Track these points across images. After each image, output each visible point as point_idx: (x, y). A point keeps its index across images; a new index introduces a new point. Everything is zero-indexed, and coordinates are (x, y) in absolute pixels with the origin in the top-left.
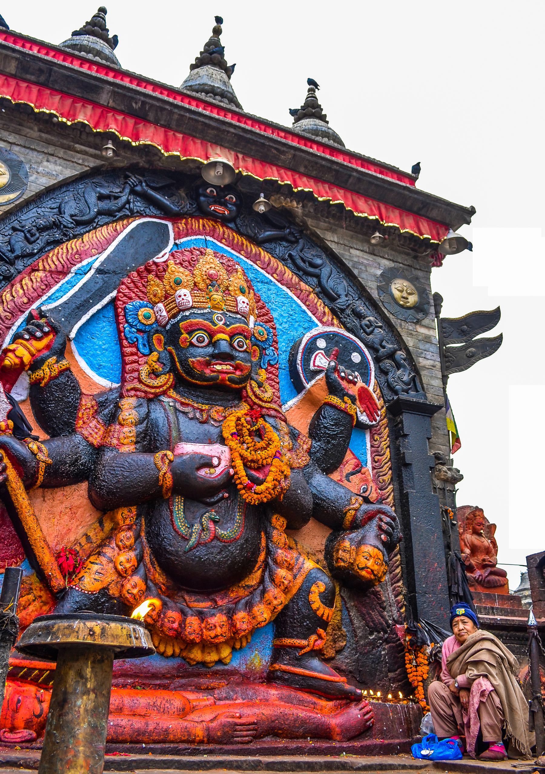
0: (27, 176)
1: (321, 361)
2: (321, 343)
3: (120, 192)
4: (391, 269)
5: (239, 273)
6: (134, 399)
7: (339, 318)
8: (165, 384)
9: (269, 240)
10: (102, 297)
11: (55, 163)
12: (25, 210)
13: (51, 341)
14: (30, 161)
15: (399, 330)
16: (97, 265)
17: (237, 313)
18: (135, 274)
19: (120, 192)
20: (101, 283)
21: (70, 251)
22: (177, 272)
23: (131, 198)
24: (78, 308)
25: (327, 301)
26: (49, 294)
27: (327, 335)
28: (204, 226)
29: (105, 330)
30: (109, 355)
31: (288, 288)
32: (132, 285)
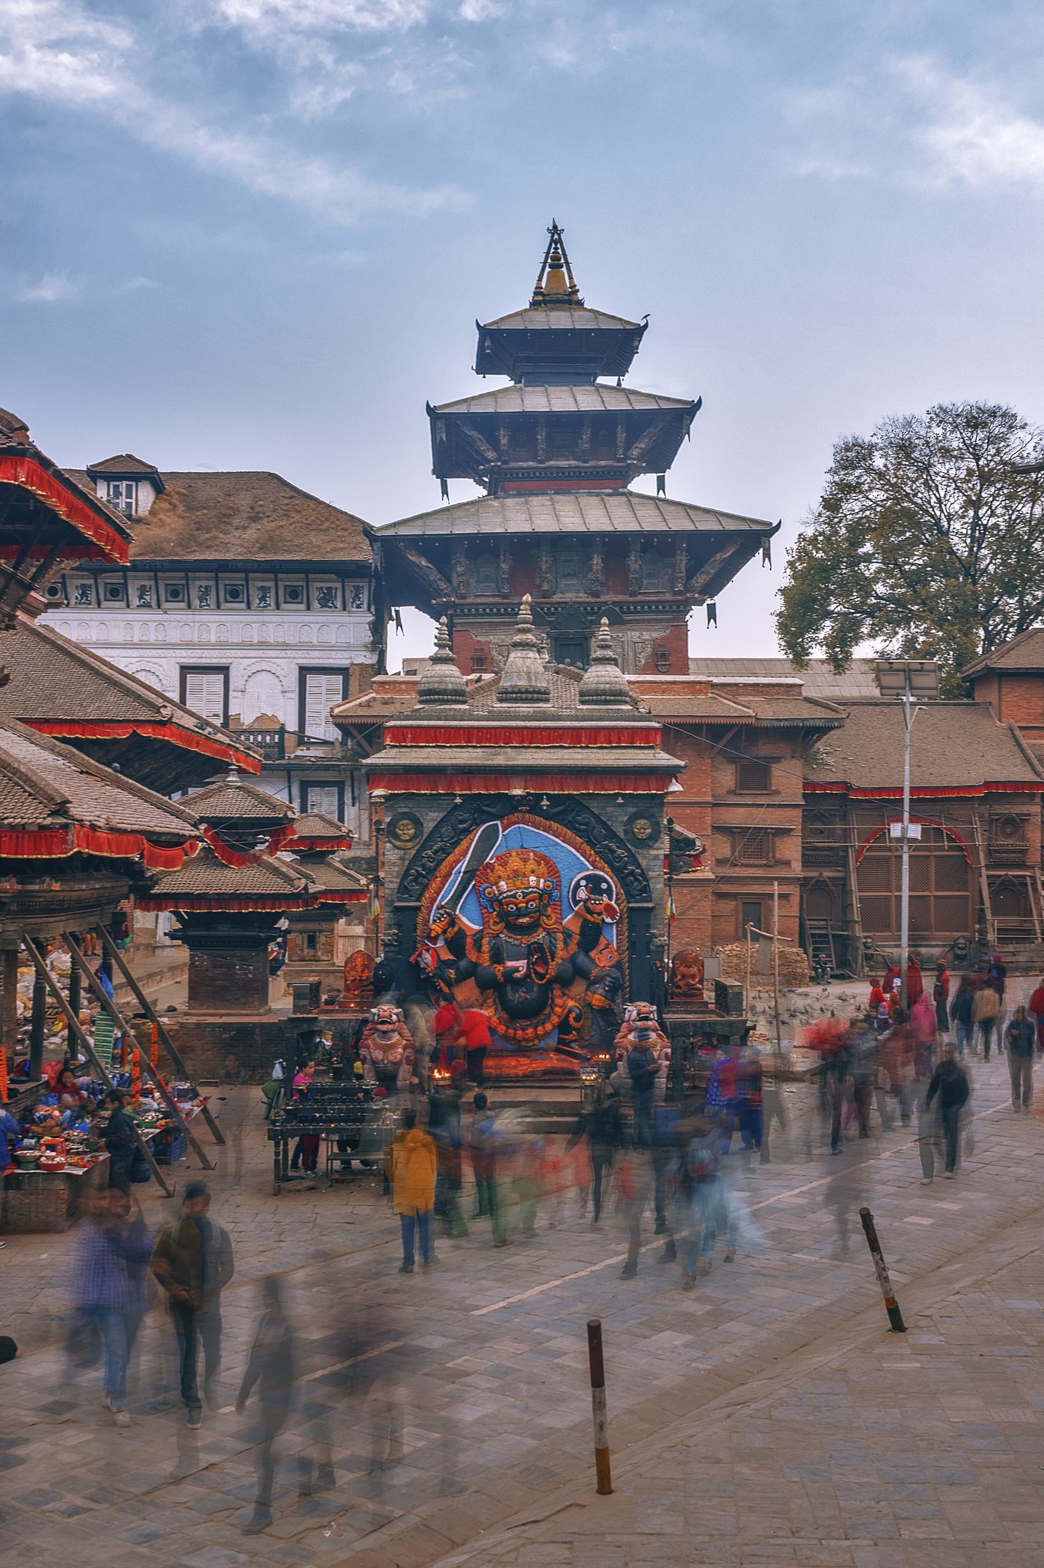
0: (422, 825)
1: (582, 894)
2: (583, 883)
4: (634, 814)
9: (558, 813)
16: (463, 870)
22: (500, 870)
29: (473, 899)
30: (476, 913)
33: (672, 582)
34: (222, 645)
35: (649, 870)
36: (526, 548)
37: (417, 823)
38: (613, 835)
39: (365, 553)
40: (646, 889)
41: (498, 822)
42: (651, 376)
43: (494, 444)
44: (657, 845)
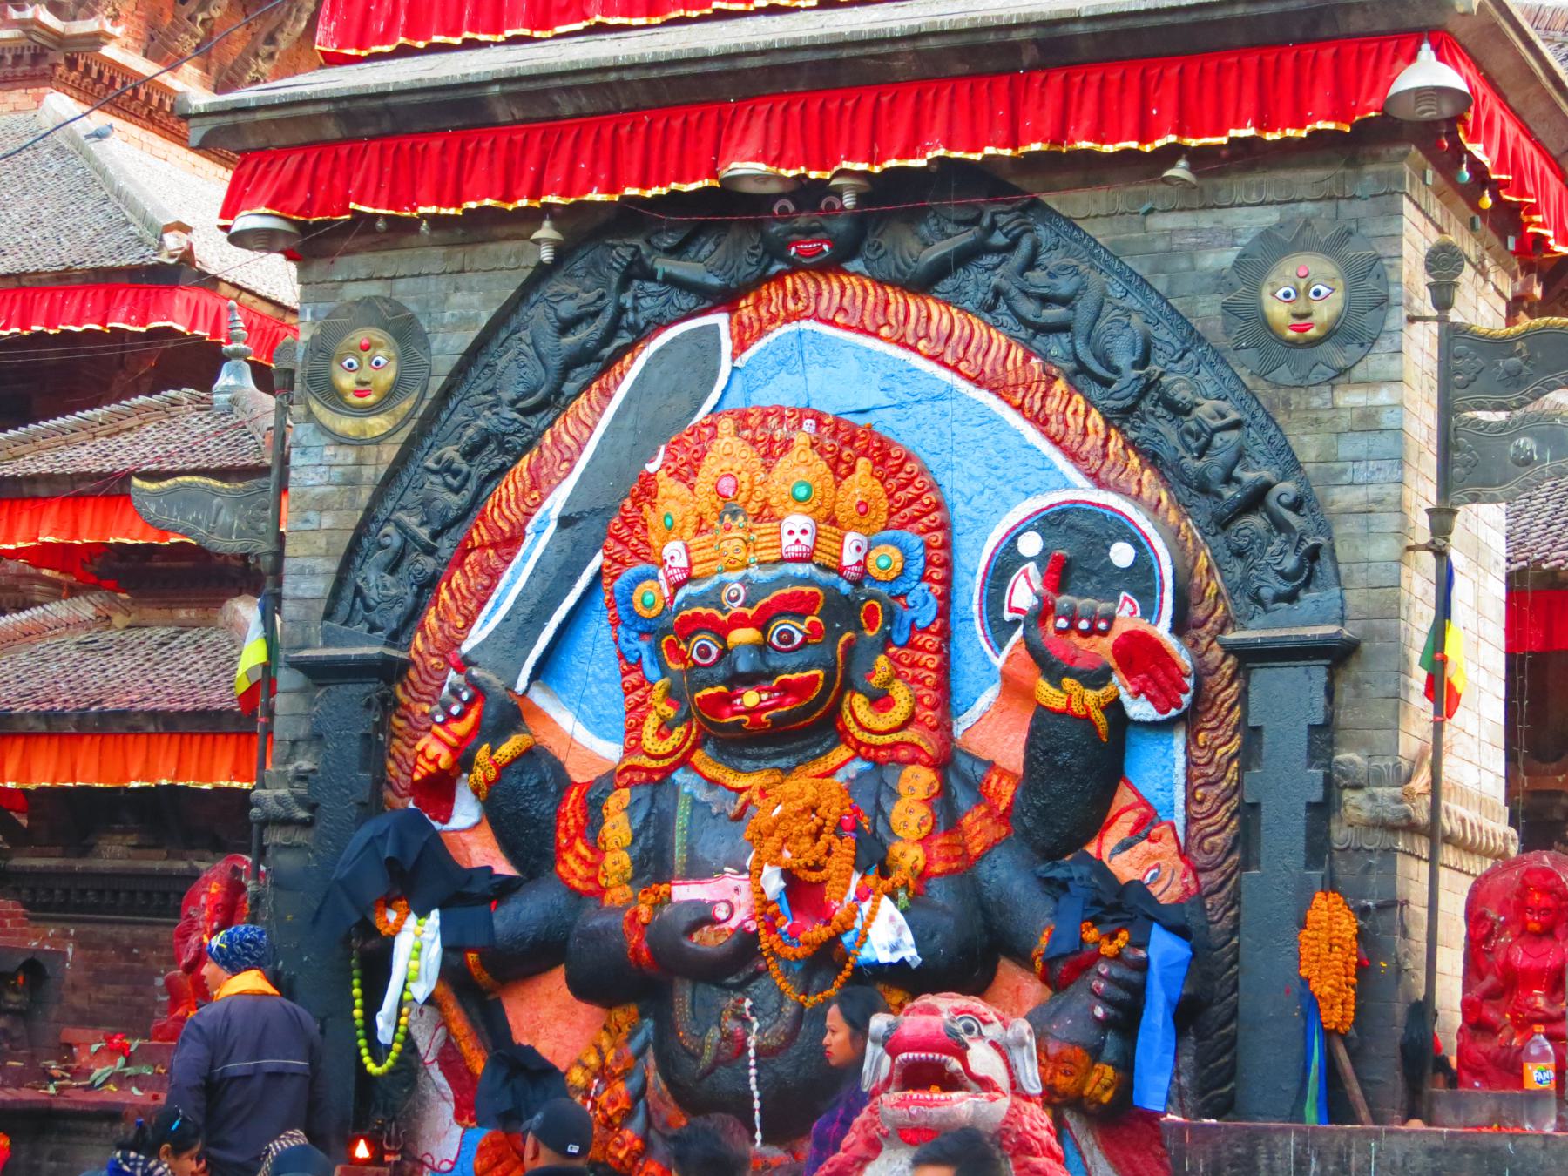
1: (1023, 593)
2: (1031, 544)
3: (601, 297)
4: (1266, 235)
5: (797, 450)
6: (626, 792)
7: (1118, 429)
8: (685, 741)
10: (573, 579)
11: (471, 290)
12: (444, 416)
13: (481, 711)
14: (427, 304)
15: (1281, 419)
17: (782, 560)
18: (628, 503)
19: (601, 297)
20: (567, 547)
21: (520, 485)
23: (626, 299)
24: (528, 621)
25: (1096, 391)
26: (494, 597)
27: (1045, 518)
28: (795, 291)
30: (610, 696)
31: (991, 390)
32: (625, 532)
35: (1333, 479)
37: (406, 331)
40: (1312, 565)
41: (721, 320)
44: (1375, 362)
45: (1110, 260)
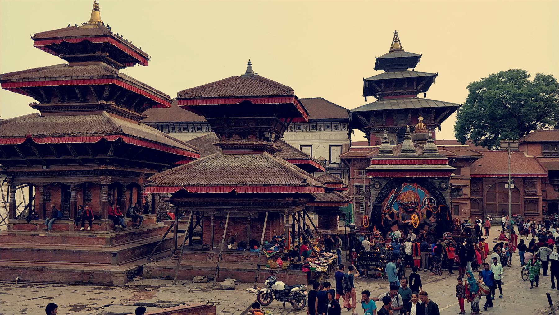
29: (396, 204)
33: (431, 120)
34: (310, 140)
36: (389, 113)
38: (435, 188)
39: (346, 116)
42: (421, 68)
43: (381, 87)
45: (430, 183)
